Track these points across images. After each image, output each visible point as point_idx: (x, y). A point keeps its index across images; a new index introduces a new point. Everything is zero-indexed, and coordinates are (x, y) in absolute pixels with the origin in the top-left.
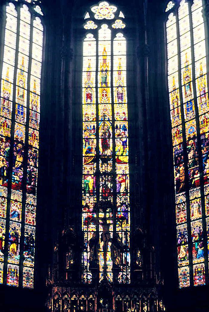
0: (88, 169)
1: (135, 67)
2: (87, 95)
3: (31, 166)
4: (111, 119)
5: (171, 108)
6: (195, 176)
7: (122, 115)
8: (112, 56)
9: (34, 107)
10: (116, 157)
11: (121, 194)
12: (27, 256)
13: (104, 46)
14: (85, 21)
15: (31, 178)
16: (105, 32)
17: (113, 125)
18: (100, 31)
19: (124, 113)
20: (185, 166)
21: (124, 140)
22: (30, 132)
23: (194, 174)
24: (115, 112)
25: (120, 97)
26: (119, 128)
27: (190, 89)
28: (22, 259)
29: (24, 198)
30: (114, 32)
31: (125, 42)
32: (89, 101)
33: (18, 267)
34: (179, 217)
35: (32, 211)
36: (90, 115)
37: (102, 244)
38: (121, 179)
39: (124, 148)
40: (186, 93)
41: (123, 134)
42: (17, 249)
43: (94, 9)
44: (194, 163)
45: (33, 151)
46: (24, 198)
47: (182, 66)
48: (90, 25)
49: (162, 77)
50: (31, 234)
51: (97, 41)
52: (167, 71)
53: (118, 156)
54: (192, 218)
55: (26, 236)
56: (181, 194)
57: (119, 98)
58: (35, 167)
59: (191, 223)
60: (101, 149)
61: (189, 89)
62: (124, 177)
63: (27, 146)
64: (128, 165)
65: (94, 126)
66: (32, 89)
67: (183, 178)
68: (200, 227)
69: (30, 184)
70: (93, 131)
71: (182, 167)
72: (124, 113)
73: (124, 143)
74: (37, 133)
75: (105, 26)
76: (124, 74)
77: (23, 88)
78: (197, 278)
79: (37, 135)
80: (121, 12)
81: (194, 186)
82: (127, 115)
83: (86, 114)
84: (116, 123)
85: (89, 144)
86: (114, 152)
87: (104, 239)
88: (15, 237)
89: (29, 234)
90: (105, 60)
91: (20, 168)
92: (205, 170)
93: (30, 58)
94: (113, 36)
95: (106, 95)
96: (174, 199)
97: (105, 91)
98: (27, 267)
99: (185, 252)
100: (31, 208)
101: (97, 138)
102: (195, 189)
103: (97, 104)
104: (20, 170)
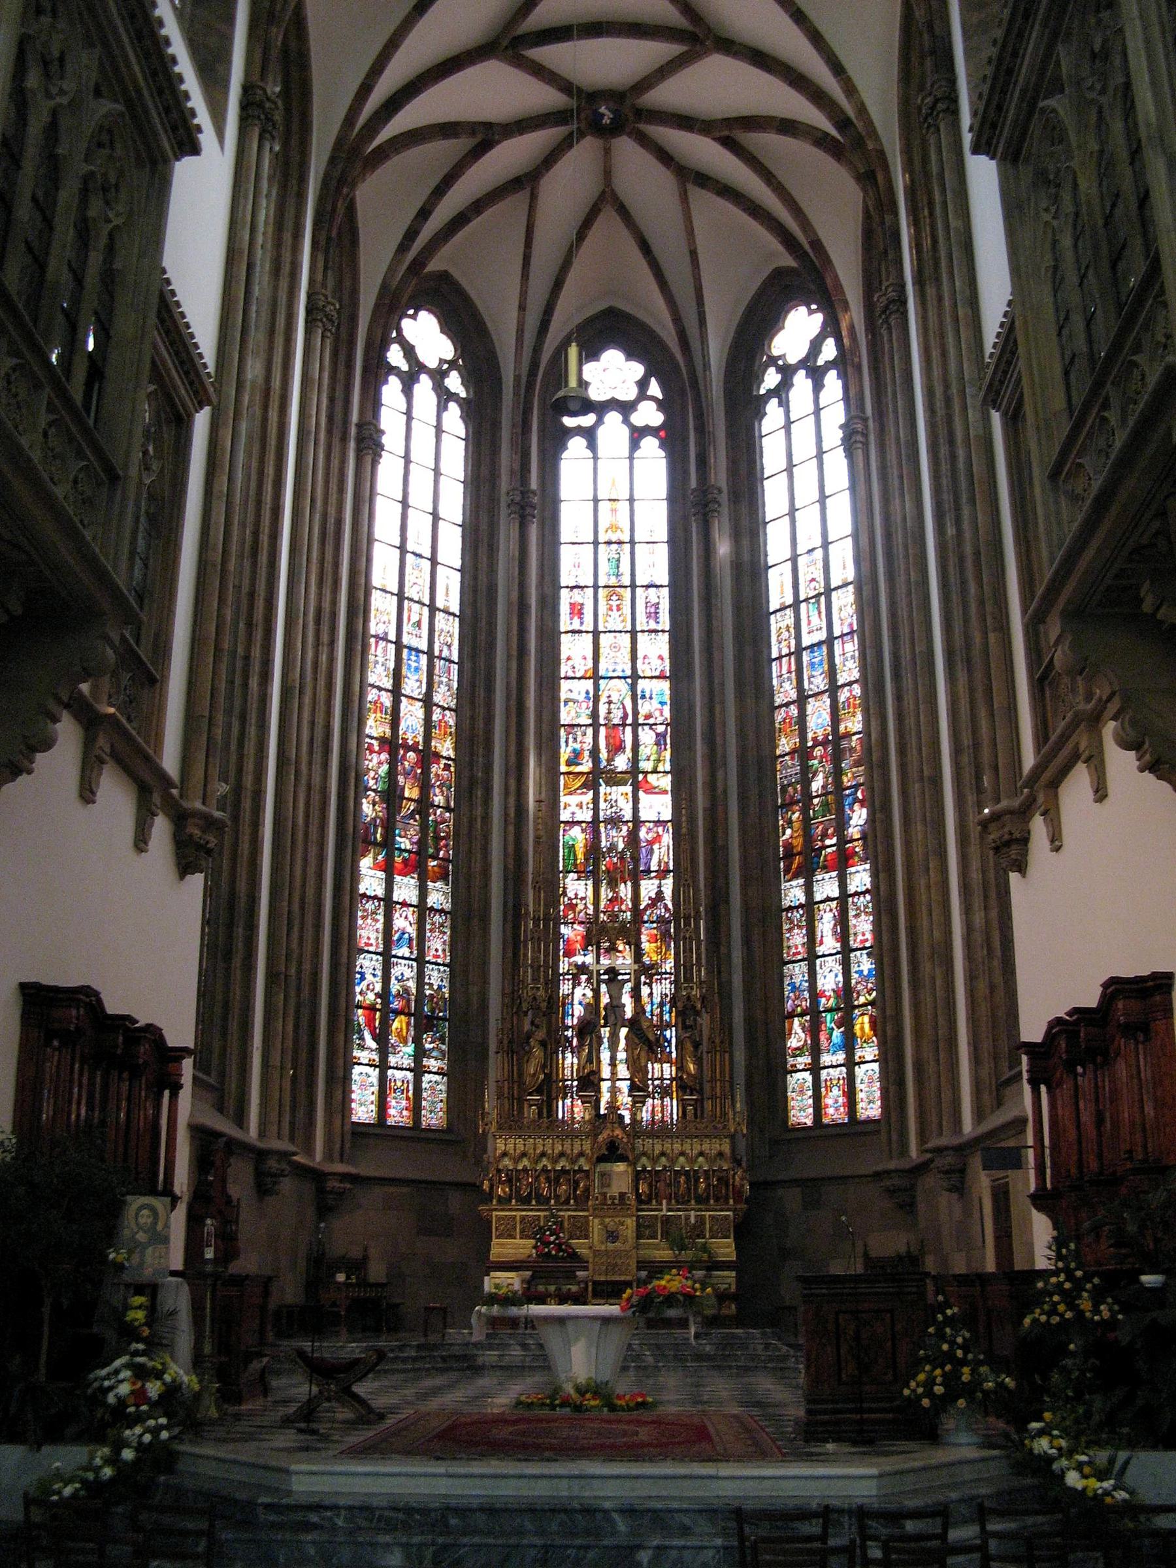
0: (574, 806)
1: (687, 530)
2: (572, 606)
3: (439, 807)
4: (628, 673)
5: (774, 655)
6: (828, 842)
7: (656, 663)
8: (631, 500)
9: (445, 648)
10: (641, 777)
11: (653, 875)
12: (431, 1046)
15: (437, 838)
17: (633, 687)
18: (601, 432)
19: (661, 658)
21: (661, 729)
22: (435, 717)
23: (825, 835)
24: (640, 655)
25: (654, 615)
26: (648, 696)
27: (820, 613)
28: (420, 1053)
29: (423, 893)
30: (638, 434)
32: (576, 621)
33: (410, 1075)
34: (791, 943)
35: (442, 925)
37: (605, 1032)
38: (650, 837)
39: (659, 753)
40: (809, 623)
41: (657, 714)
42: (408, 1030)
45: (442, 766)
46: (423, 893)
49: (751, 571)
50: (440, 987)
51: (595, 458)
52: (766, 555)
53: (647, 773)
54: (820, 950)
55: (428, 992)
56: (794, 883)
57: (649, 615)
58: (447, 808)
59: (818, 962)
60: (604, 755)
61: (816, 612)
62: (660, 829)
63: (427, 756)
64: (668, 799)
65: (587, 692)
66: (440, 604)
67: (798, 843)
68: (836, 976)
70: (584, 705)
71: (797, 814)
72: (661, 658)
75: (613, 418)
76: (663, 551)
78: (829, 1101)
79: (452, 722)
80: (653, 380)
81: (826, 869)
82: (667, 662)
83: (569, 659)
84: (642, 684)
85: (575, 739)
86: (635, 759)
87: (612, 1019)
88: (403, 998)
89: (435, 987)
92: (850, 830)
93: (436, 517)
94: (635, 444)
95: (618, 609)
97: (614, 598)
98: (430, 1072)
99: (803, 1035)
100: (438, 919)
101: (595, 725)
102: (827, 876)
103: (596, 634)
104: (412, 821)
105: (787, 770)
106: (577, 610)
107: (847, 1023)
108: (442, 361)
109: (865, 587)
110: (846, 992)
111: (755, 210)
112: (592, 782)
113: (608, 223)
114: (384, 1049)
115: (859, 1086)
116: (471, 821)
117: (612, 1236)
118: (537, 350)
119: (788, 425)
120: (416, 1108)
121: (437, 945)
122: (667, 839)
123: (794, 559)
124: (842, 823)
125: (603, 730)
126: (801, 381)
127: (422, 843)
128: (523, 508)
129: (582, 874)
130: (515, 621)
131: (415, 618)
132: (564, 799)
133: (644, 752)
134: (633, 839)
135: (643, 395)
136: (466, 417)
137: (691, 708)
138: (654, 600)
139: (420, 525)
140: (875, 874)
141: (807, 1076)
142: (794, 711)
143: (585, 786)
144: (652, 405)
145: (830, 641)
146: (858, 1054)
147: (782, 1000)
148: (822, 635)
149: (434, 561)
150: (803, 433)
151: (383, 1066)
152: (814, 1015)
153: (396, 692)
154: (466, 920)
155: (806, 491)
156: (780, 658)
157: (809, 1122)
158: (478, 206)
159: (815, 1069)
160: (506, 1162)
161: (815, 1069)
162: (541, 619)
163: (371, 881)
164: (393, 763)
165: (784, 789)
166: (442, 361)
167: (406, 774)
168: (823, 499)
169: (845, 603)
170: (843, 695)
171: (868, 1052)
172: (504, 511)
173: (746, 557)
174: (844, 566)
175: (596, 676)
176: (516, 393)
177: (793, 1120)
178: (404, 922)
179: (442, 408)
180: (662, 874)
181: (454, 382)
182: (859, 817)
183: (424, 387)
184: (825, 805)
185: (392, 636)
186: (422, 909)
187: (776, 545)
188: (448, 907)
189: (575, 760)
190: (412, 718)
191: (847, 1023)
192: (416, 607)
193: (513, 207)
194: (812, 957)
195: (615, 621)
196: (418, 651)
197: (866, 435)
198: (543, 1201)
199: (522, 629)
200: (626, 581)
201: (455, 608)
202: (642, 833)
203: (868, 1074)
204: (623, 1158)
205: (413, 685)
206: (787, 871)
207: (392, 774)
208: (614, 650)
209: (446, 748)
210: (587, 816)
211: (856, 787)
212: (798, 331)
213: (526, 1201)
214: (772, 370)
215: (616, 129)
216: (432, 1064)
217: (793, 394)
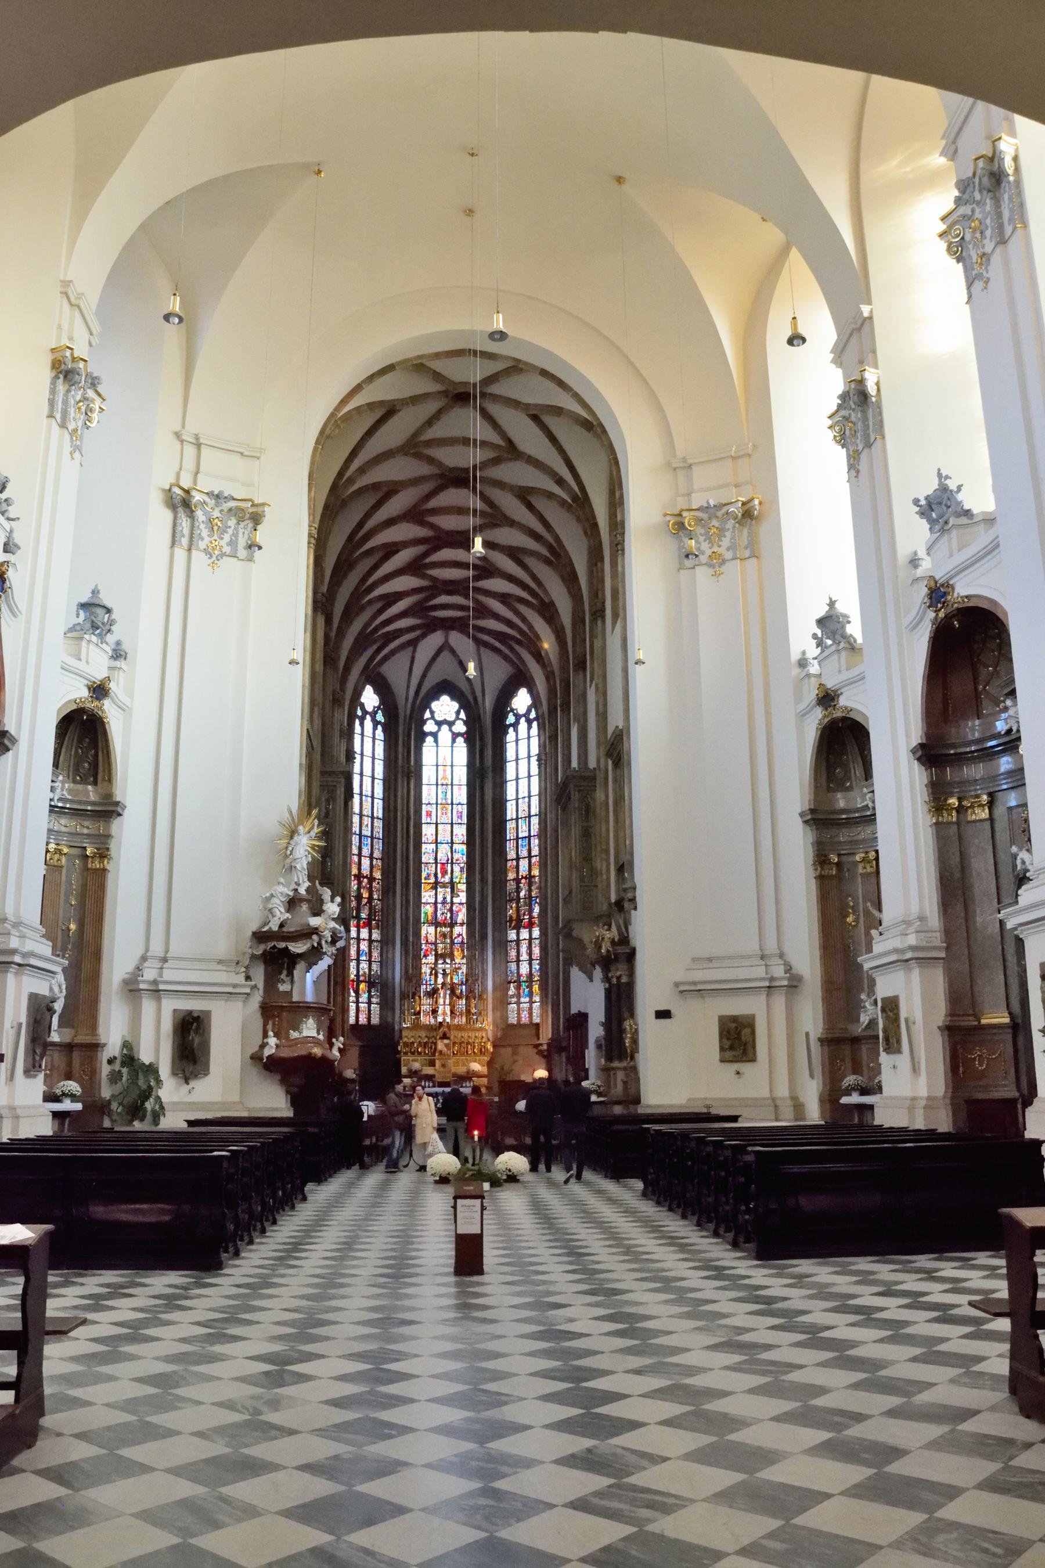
0: (427, 896)
7: (461, 837)
8: (452, 766)
13: (445, 751)
14: (424, 722)
16: (445, 734)
17: (451, 848)
18: (440, 734)
25: (460, 817)
28: (370, 997)
30: (455, 736)
31: (465, 749)
36: (429, 834)
43: (435, 705)
44: (525, 904)
47: (520, 796)
48: (430, 727)
49: (500, 802)
54: (521, 958)
60: (439, 875)
63: (371, 879)
66: (375, 815)
67: (514, 916)
73: (462, 869)
74: (379, 863)
75: (445, 728)
76: (464, 789)
81: (525, 927)
84: (455, 846)
90: (445, 771)
94: (454, 741)
101: (436, 863)
103: (437, 824)
105: (511, 886)
107: (530, 987)
109: (542, 815)
110: (530, 975)
111: (506, 658)
112: (435, 886)
116: (388, 906)
117: (444, 1066)
119: (517, 741)
120: (369, 1018)
121: (376, 954)
122: (464, 910)
123: (517, 799)
124: (531, 911)
126: (523, 720)
129: (431, 924)
133: (455, 875)
134: (451, 910)
135: (457, 718)
136: (384, 731)
139: (367, 781)
140: (541, 935)
142: (514, 862)
144: (461, 722)
145: (529, 837)
149: (373, 797)
150: (523, 744)
151: (357, 1002)
152: (518, 982)
153: (360, 855)
154: (386, 942)
155: (523, 773)
158: (393, 653)
159: (518, 1003)
160: (405, 1040)
161: (518, 1003)
162: (415, 820)
163: (353, 933)
164: (360, 883)
168: (529, 776)
169: (535, 821)
170: (534, 860)
171: (537, 998)
172: (399, 776)
174: (535, 810)
175: (436, 842)
176: (405, 720)
178: (364, 946)
179: (375, 729)
180: (462, 924)
181: (380, 717)
182: (537, 910)
183: (368, 723)
186: (371, 941)
189: (428, 877)
190: (366, 863)
191: (530, 987)
194: (518, 961)
195: (446, 819)
198: (419, 1053)
201: (381, 816)
202: (454, 908)
204: (448, 1038)
205: (366, 851)
207: (359, 889)
209: (378, 875)
210: (433, 901)
212: (522, 700)
213: (413, 1053)
215: (452, 628)
216: (374, 1000)
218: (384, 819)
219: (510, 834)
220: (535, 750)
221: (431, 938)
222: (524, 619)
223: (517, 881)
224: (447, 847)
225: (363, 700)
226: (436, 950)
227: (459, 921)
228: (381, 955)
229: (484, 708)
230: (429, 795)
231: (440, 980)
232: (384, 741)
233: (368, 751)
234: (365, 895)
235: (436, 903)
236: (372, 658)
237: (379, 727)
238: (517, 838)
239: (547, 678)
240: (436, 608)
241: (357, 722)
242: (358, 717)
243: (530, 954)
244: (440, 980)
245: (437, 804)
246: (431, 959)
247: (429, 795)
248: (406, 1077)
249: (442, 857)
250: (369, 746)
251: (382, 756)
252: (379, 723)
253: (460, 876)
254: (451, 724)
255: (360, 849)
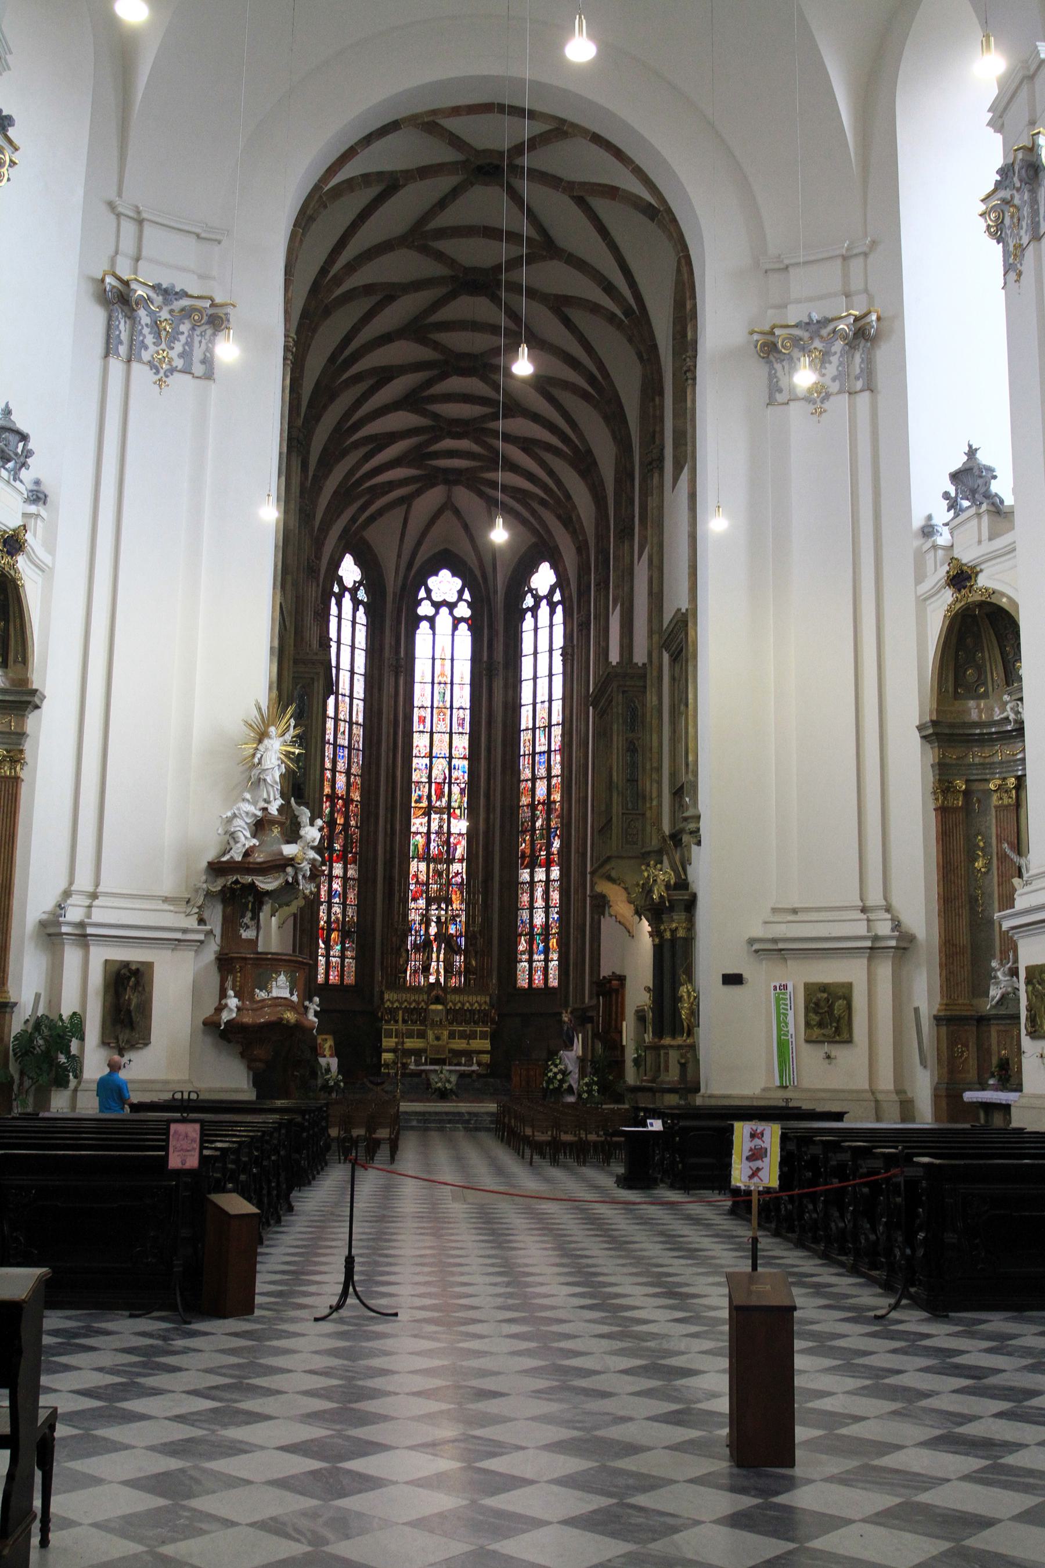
0: (418, 824)
1: (481, 680)
2: (420, 718)
5: (522, 753)
7: (461, 750)
8: (452, 660)
14: (419, 603)
15: (352, 842)
16: (444, 619)
17: (450, 763)
18: (438, 618)
20: (532, 836)
21: (463, 786)
24: (454, 746)
25: (462, 725)
28: (343, 950)
30: (457, 622)
31: (469, 639)
32: (422, 726)
39: (461, 798)
43: (432, 582)
44: (542, 836)
47: (538, 700)
48: (425, 609)
51: (434, 634)
54: (536, 905)
57: (459, 725)
58: (356, 827)
60: (434, 798)
63: (348, 801)
66: (354, 720)
67: (528, 851)
69: (351, 852)
73: (462, 791)
75: (444, 611)
76: (467, 689)
77: (345, 721)
81: (540, 866)
84: (454, 762)
90: (443, 665)
91: (340, 833)
94: (455, 628)
96: (517, 876)
101: (430, 782)
103: (432, 733)
105: (525, 813)
106: (422, 720)
108: (355, 582)
109: (567, 724)
110: (546, 926)
111: (524, 522)
112: (428, 812)
113: (448, 514)
114: (328, 948)
115: (550, 971)
117: (438, 1038)
118: (406, 577)
119: (536, 629)
120: (342, 976)
121: (351, 896)
122: (464, 843)
123: (534, 704)
124: (549, 845)
125: (433, 785)
126: (544, 602)
127: (345, 846)
128: (397, 668)
130: (392, 731)
131: (342, 730)
132: (413, 821)
134: (447, 842)
135: (460, 598)
137: (479, 777)
138: (462, 716)
141: (526, 964)
142: (529, 784)
143: (424, 814)
145: (549, 751)
146: (551, 956)
147: (517, 927)
148: (545, 748)
149: (351, 697)
151: (327, 956)
153: (334, 770)
156: (524, 755)
157: (526, 986)
158: (380, 513)
159: (530, 961)
161: (530, 961)
162: (404, 726)
164: (333, 806)
165: (523, 823)
166: (355, 582)
167: (338, 812)
168: (551, 675)
169: (557, 731)
170: (554, 781)
171: (555, 956)
172: (386, 669)
173: (510, 699)
174: (557, 717)
175: (431, 756)
177: (519, 985)
178: (337, 886)
179: (355, 610)
180: (461, 861)
181: (362, 595)
182: (556, 844)
183: (347, 602)
184: (542, 835)
185: (332, 741)
186: (345, 879)
187: (526, 696)
188: (356, 876)
189: (419, 800)
190: (341, 780)
191: (546, 941)
192: (342, 724)
193: (399, 513)
194: (532, 908)
195: (441, 726)
196: (343, 747)
197: (572, 655)
199: (396, 733)
200: (448, 706)
201: (361, 721)
202: (452, 840)
203: (554, 964)
205: (341, 765)
206: (522, 864)
207: (332, 813)
208: (440, 745)
209: (356, 796)
210: (425, 830)
211: (557, 828)
212: (544, 578)
214: (529, 595)
215: (456, 482)
216: (348, 953)
217: (540, 612)
218: (364, 726)
219: (525, 748)
220: (559, 641)
221: (423, 877)
222: (551, 473)
223: (533, 806)
224: (444, 763)
225: (341, 573)
226: (427, 892)
227: (458, 855)
228: (359, 895)
229: (495, 586)
230: (423, 695)
231: (433, 930)
232: (367, 626)
233: (346, 638)
234: (340, 820)
235: (429, 833)
236: (353, 519)
237: (361, 608)
238: (534, 754)
239: (579, 550)
240: (437, 455)
241: (333, 601)
242: (334, 594)
243: (547, 898)
244: (433, 930)
245: (432, 707)
246: (422, 903)
247: (423, 695)
248: (388, 1051)
249: (438, 774)
250: (348, 632)
251: (363, 646)
252: (361, 602)
253: (457, 797)
254: (452, 606)
255: (334, 762)
